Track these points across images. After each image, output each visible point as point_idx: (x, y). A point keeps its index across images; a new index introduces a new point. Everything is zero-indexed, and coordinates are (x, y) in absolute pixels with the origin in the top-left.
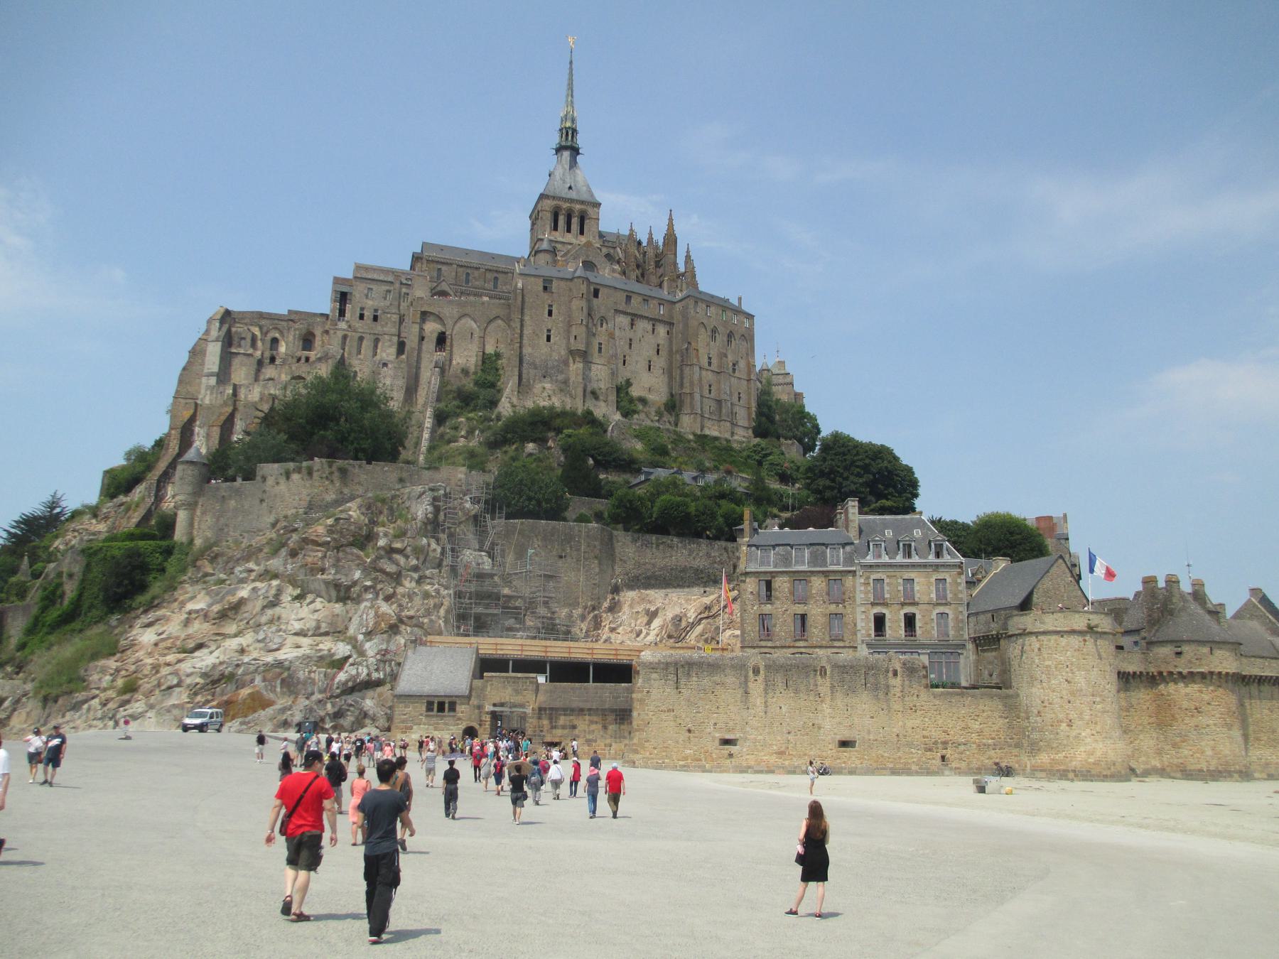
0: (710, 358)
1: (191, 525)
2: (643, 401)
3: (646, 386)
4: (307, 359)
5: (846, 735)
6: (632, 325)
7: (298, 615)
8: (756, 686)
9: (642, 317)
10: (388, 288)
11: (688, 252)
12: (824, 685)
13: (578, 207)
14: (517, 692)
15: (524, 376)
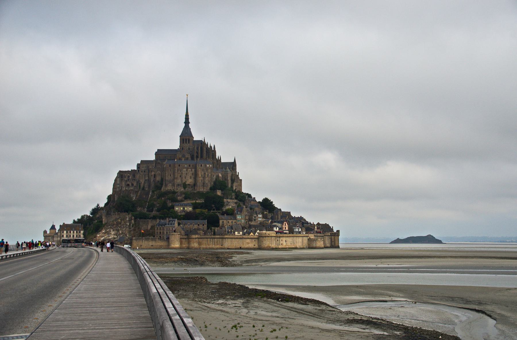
0: (202, 175)
1: (104, 221)
2: (189, 185)
3: (190, 182)
4: (134, 180)
5: (152, 245)
6: (187, 170)
7: (113, 233)
8: (144, 241)
9: (188, 168)
10: (146, 165)
11: (210, 145)
12: (150, 240)
13: (188, 137)
14: (127, 241)
15: (166, 183)
